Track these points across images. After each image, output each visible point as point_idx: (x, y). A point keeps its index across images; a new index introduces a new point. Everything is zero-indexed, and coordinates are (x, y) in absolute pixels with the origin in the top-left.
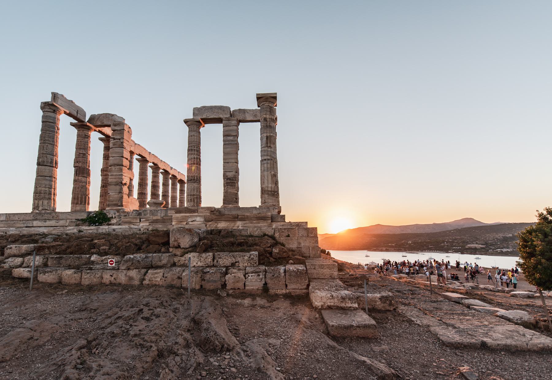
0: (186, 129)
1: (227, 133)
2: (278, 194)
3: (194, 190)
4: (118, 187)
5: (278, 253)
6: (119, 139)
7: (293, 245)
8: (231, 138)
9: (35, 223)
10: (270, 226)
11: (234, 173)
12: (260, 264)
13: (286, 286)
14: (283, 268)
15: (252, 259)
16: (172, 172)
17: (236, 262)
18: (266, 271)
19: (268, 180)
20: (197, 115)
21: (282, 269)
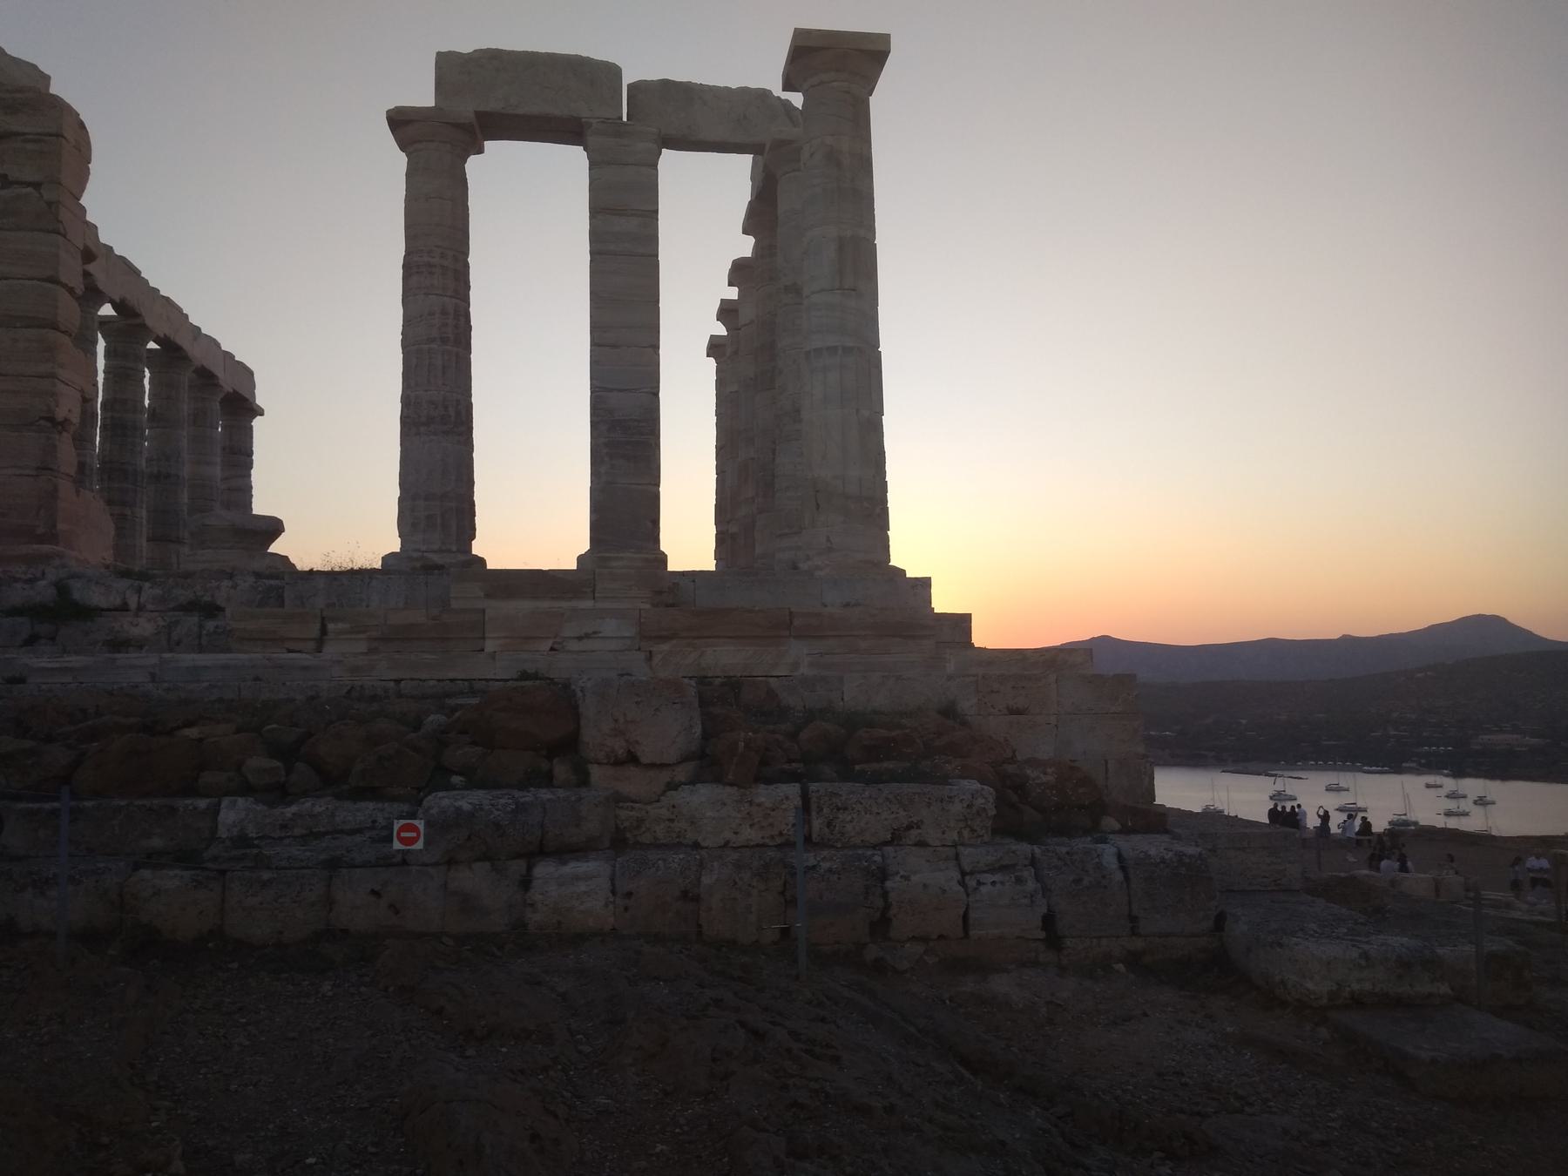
16: (195, 352)
17: (909, 827)
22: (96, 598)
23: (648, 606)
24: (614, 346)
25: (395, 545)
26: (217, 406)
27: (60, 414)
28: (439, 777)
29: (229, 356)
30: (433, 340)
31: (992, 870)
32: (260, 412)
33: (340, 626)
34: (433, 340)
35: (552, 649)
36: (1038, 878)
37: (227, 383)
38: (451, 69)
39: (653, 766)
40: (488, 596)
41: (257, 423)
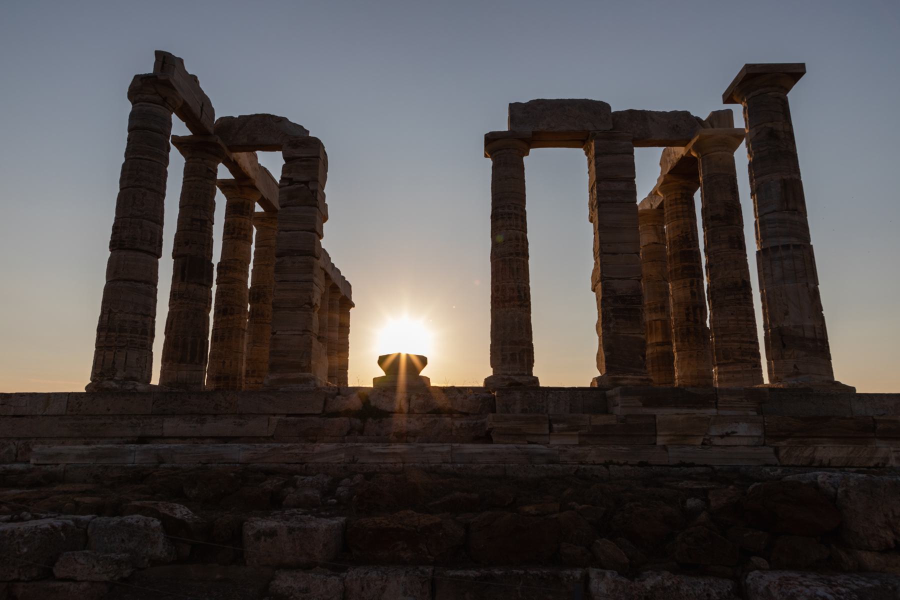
6: (306, 183)
9: (170, 426)
23: (755, 413)
24: (614, 254)
25: (490, 372)
26: (338, 302)
29: (343, 278)
30: (511, 254)
32: (353, 305)
33: (561, 426)
34: (511, 254)
35: (703, 444)
38: (517, 111)
40: (645, 405)
41: (352, 311)
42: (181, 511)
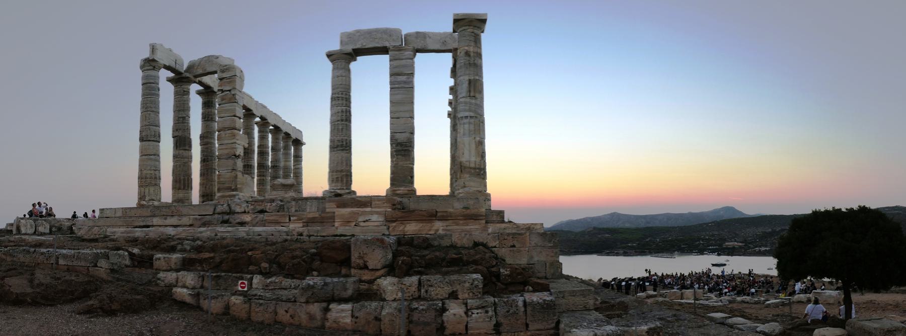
0: (329, 65)
1: (396, 70)
2: (485, 173)
3: (342, 163)
4: (230, 162)
5: (509, 276)
7: (523, 261)
8: (403, 78)
10: (485, 229)
11: (407, 135)
12: (484, 293)
13: (527, 325)
14: (521, 299)
15: (476, 286)
18: (495, 304)
19: (470, 151)
20: (347, 44)
21: (520, 300)
22: (238, 209)
27: (237, 153)
28: (308, 272)
31: (477, 309)
36: (495, 311)
37: (294, 136)
39: (372, 270)
42: (136, 251)
